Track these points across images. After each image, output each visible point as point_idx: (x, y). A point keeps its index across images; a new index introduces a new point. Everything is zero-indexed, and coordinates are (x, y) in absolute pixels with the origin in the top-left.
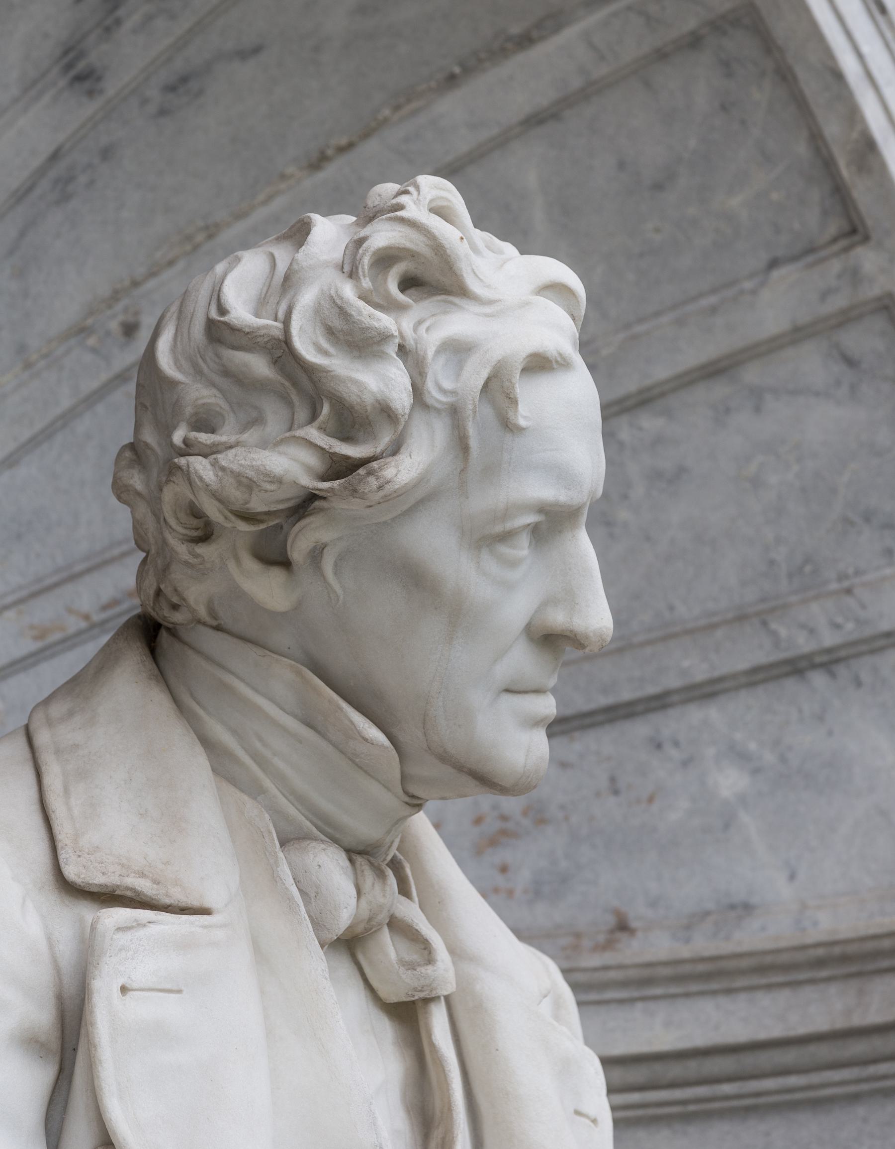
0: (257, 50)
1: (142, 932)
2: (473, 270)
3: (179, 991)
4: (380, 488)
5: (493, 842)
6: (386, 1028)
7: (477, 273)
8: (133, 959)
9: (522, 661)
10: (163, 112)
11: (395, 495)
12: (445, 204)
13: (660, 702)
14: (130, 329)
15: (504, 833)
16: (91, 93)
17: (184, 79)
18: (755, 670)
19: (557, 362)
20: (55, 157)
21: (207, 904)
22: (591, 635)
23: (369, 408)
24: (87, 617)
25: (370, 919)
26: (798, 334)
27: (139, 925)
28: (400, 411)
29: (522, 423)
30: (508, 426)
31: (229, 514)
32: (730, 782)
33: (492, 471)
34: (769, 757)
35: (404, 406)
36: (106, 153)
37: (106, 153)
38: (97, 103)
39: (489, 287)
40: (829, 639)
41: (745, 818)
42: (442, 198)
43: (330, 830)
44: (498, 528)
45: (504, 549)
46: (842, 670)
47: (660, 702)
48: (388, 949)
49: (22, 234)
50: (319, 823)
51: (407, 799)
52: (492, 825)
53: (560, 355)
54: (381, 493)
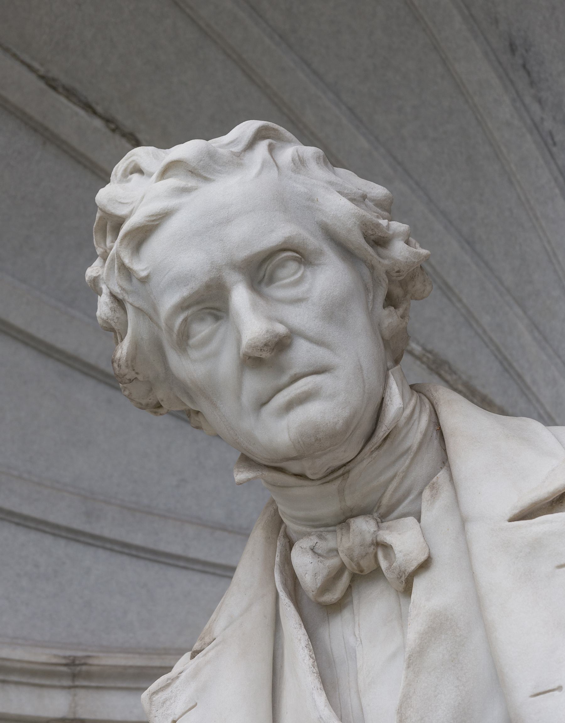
1: (178, 682)
2: (120, 203)
3: (196, 704)
4: (119, 366)
7: (123, 201)
8: (175, 701)
9: (254, 384)
11: (129, 362)
12: (133, 164)
19: (153, 221)
21: (214, 637)
22: (246, 350)
23: (104, 325)
25: (352, 559)
27: (172, 680)
28: (105, 318)
29: (143, 274)
30: (144, 281)
31: (155, 410)
33: (155, 309)
35: (105, 314)
39: (132, 203)
42: (131, 162)
43: (318, 523)
44: (175, 336)
45: (192, 341)
48: (384, 564)
50: (311, 523)
51: (319, 482)
53: (152, 216)
54: (123, 367)
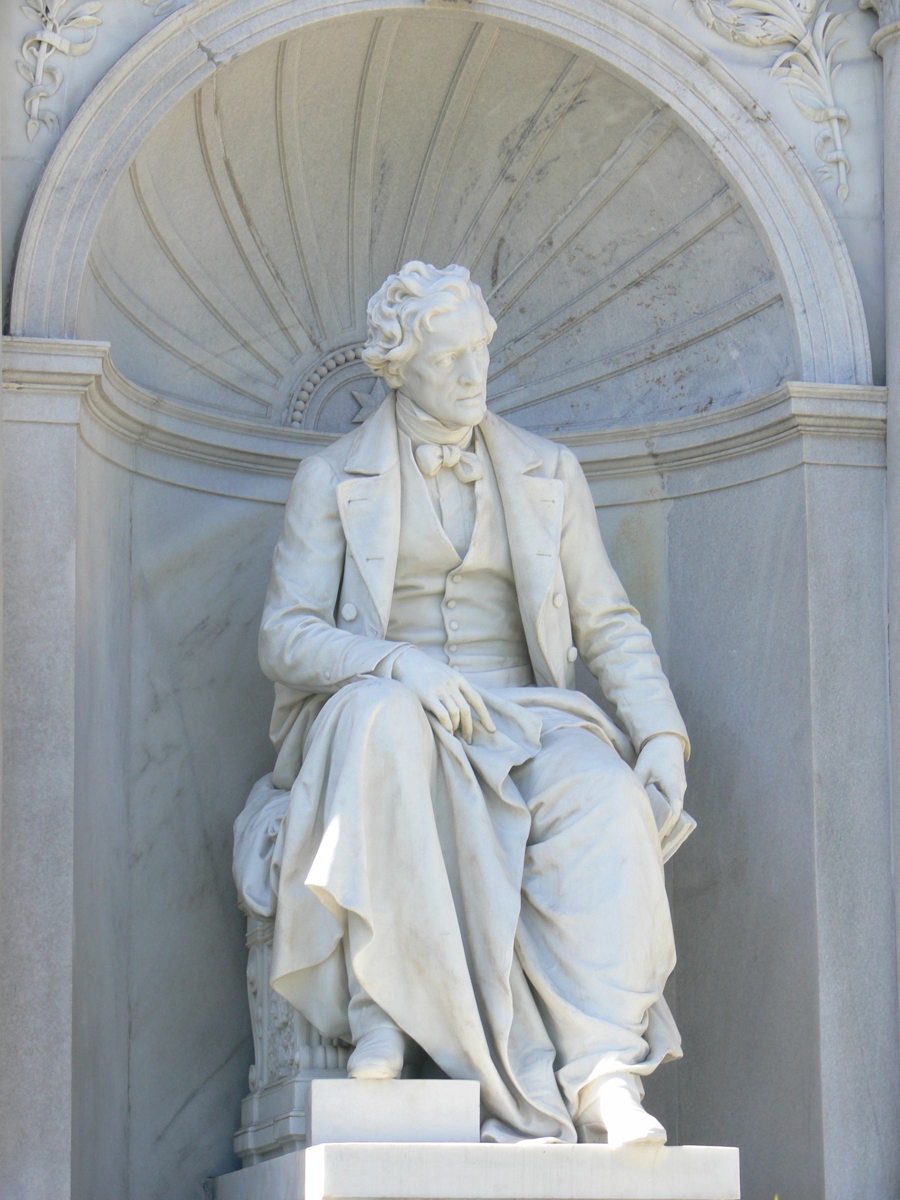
0: (558, 158)
5: (679, 380)
6: (466, 489)
10: (539, 181)
13: (716, 332)
14: (551, 243)
15: (681, 376)
16: (513, 181)
17: (541, 171)
18: (736, 319)
20: (510, 200)
24: (556, 330)
26: (724, 217)
32: (735, 354)
34: (743, 346)
36: (527, 195)
37: (527, 195)
38: (515, 184)
40: (750, 308)
41: (739, 365)
46: (756, 316)
47: (716, 332)
49: (510, 222)
52: (678, 374)
